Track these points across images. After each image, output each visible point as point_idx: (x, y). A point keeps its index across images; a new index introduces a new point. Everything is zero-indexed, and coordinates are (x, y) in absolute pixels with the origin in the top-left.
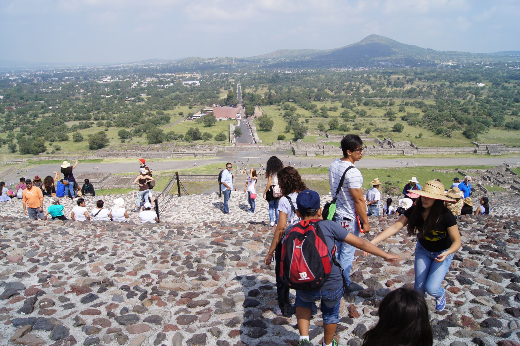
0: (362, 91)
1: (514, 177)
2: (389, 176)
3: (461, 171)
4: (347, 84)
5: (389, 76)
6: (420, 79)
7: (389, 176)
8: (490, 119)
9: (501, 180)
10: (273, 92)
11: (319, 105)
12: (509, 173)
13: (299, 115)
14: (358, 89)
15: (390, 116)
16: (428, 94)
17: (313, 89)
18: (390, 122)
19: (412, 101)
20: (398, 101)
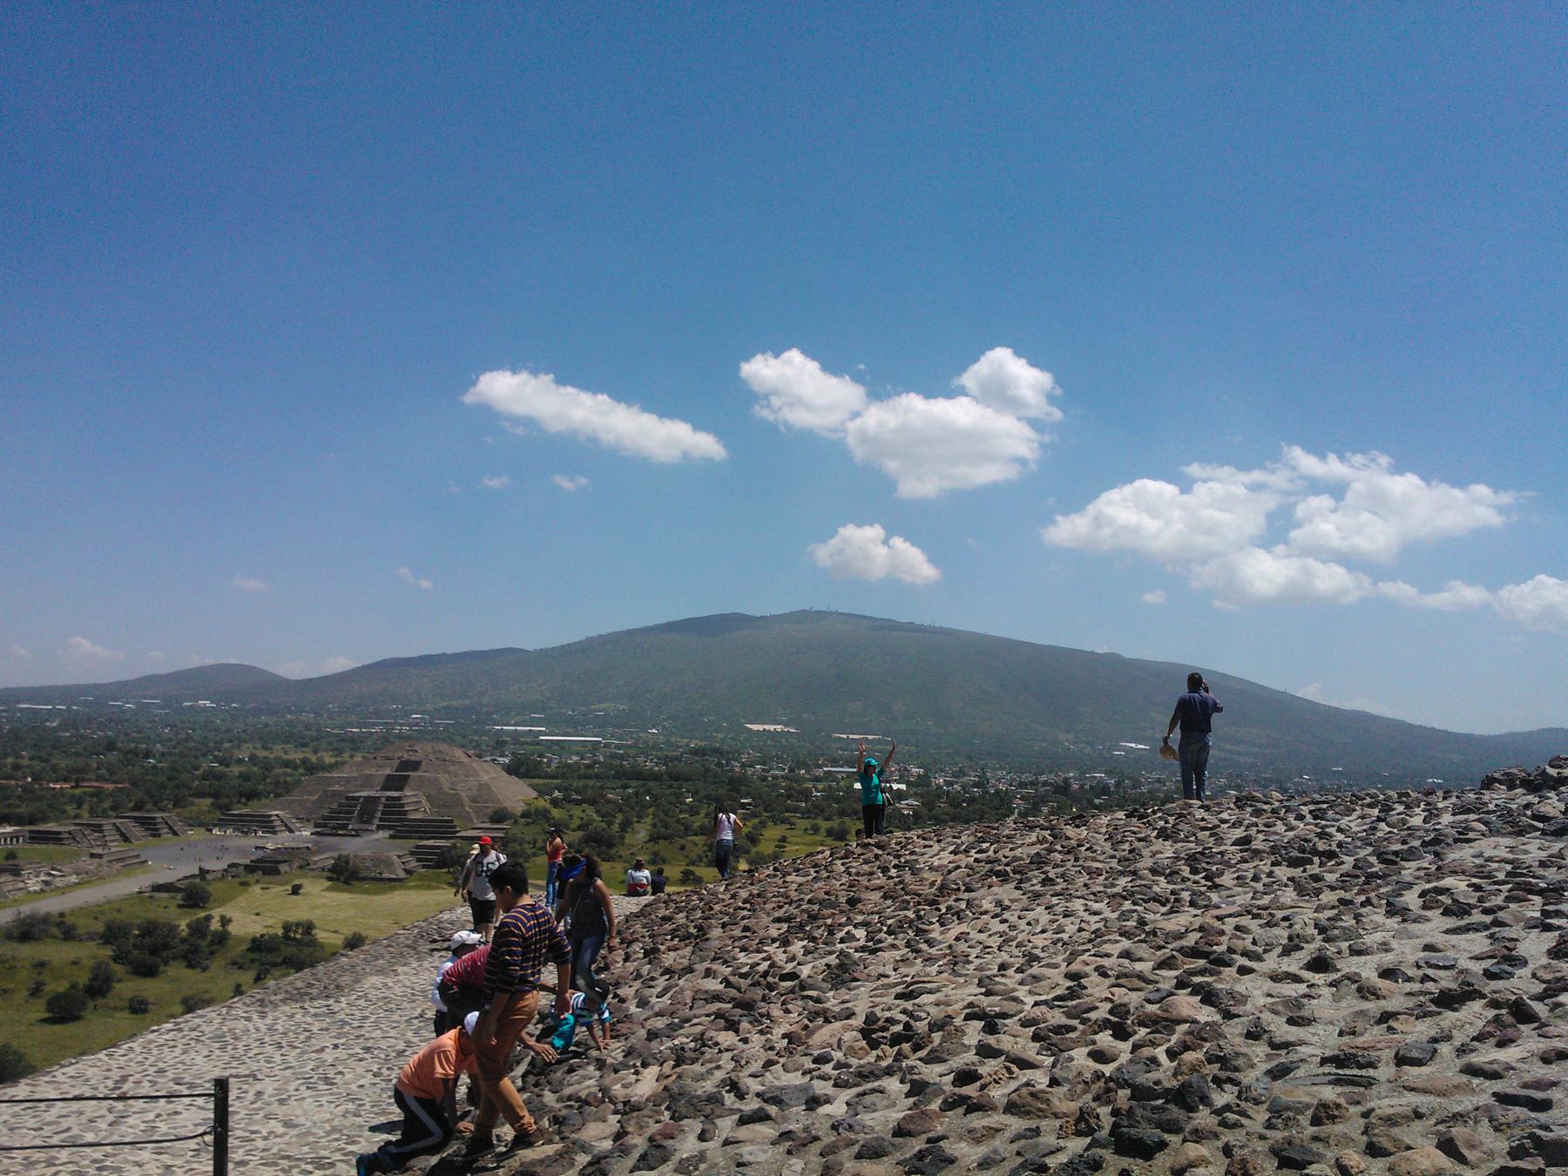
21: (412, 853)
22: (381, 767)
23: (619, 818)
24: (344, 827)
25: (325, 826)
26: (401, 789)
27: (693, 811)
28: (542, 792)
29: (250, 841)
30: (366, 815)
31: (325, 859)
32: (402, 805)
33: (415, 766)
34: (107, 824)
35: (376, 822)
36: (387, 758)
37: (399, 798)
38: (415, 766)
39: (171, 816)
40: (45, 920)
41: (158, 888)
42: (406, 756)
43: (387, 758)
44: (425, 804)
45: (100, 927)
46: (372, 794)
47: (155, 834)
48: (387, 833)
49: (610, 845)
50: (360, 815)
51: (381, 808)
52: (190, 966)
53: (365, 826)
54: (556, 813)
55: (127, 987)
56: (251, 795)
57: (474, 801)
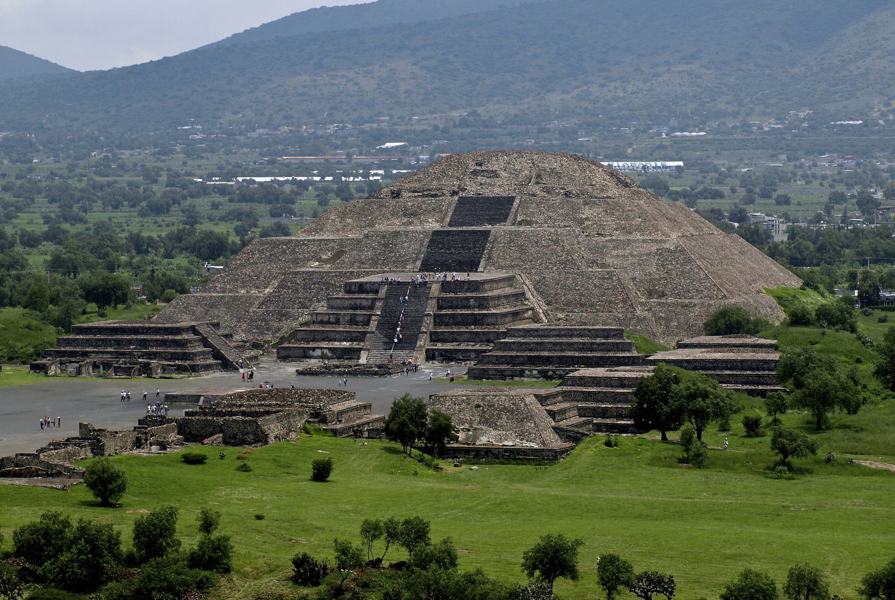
22: (411, 214)
24: (353, 353)
25: (305, 355)
26: (473, 266)
32: (483, 303)
35: (423, 342)
36: (427, 193)
37: (475, 286)
38: (499, 209)
42: (472, 189)
43: (427, 193)
44: (534, 300)
46: (411, 274)
48: (460, 370)
50: (388, 325)
51: (431, 308)
53: (401, 355)
57: (650, 294)
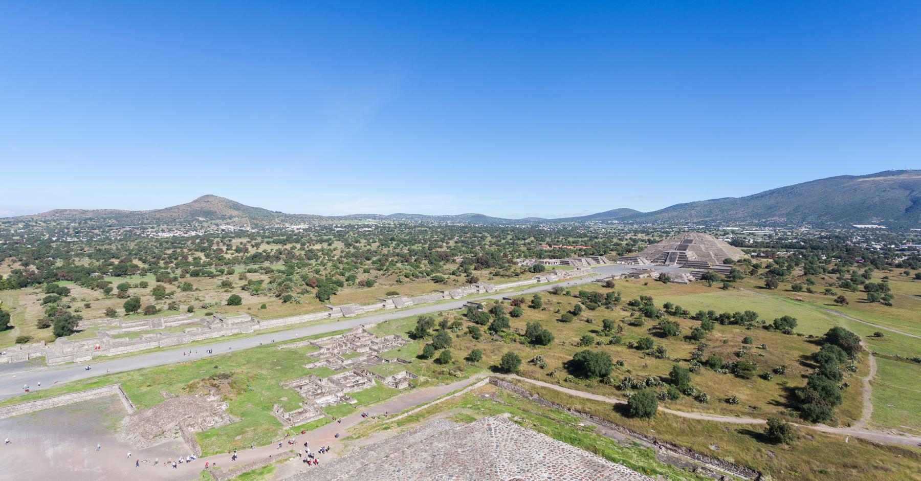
0: (190, 259)
1: (371, 337)
2: (216, 367)
3: (313, 341)
4: (170, 252)
5: (230, 241)
6: (268, 243)
7: (216, 367)
8: (342, 279)
9: (358, 344)
10: (32, 268)
11: (116, 282)
12: (365, 334)
13: (74, 299)
14: (185, 258)
15: (226, 285)
16: (278, 258)
17: (113, 260)
18: (225, 294)
19: (256, 267)
20: (239, 269)
21: (691, 273)
23: (786, 264)
27: (827, 262)
28: (746, 252)
29: (630, 266)
30: (672, 260)
31: (656, 275)
33: (691, 241)
34: (583, 260)
38: (691, 241)
39: (604, 258)
40: (562, 289)
41: (598, 281)
45: (577, 293)
47: (598, 262)
49: (782, 275)
52: (608, 308)
54: (754, 261)
55: (586, 314)
56: (630, 251)
